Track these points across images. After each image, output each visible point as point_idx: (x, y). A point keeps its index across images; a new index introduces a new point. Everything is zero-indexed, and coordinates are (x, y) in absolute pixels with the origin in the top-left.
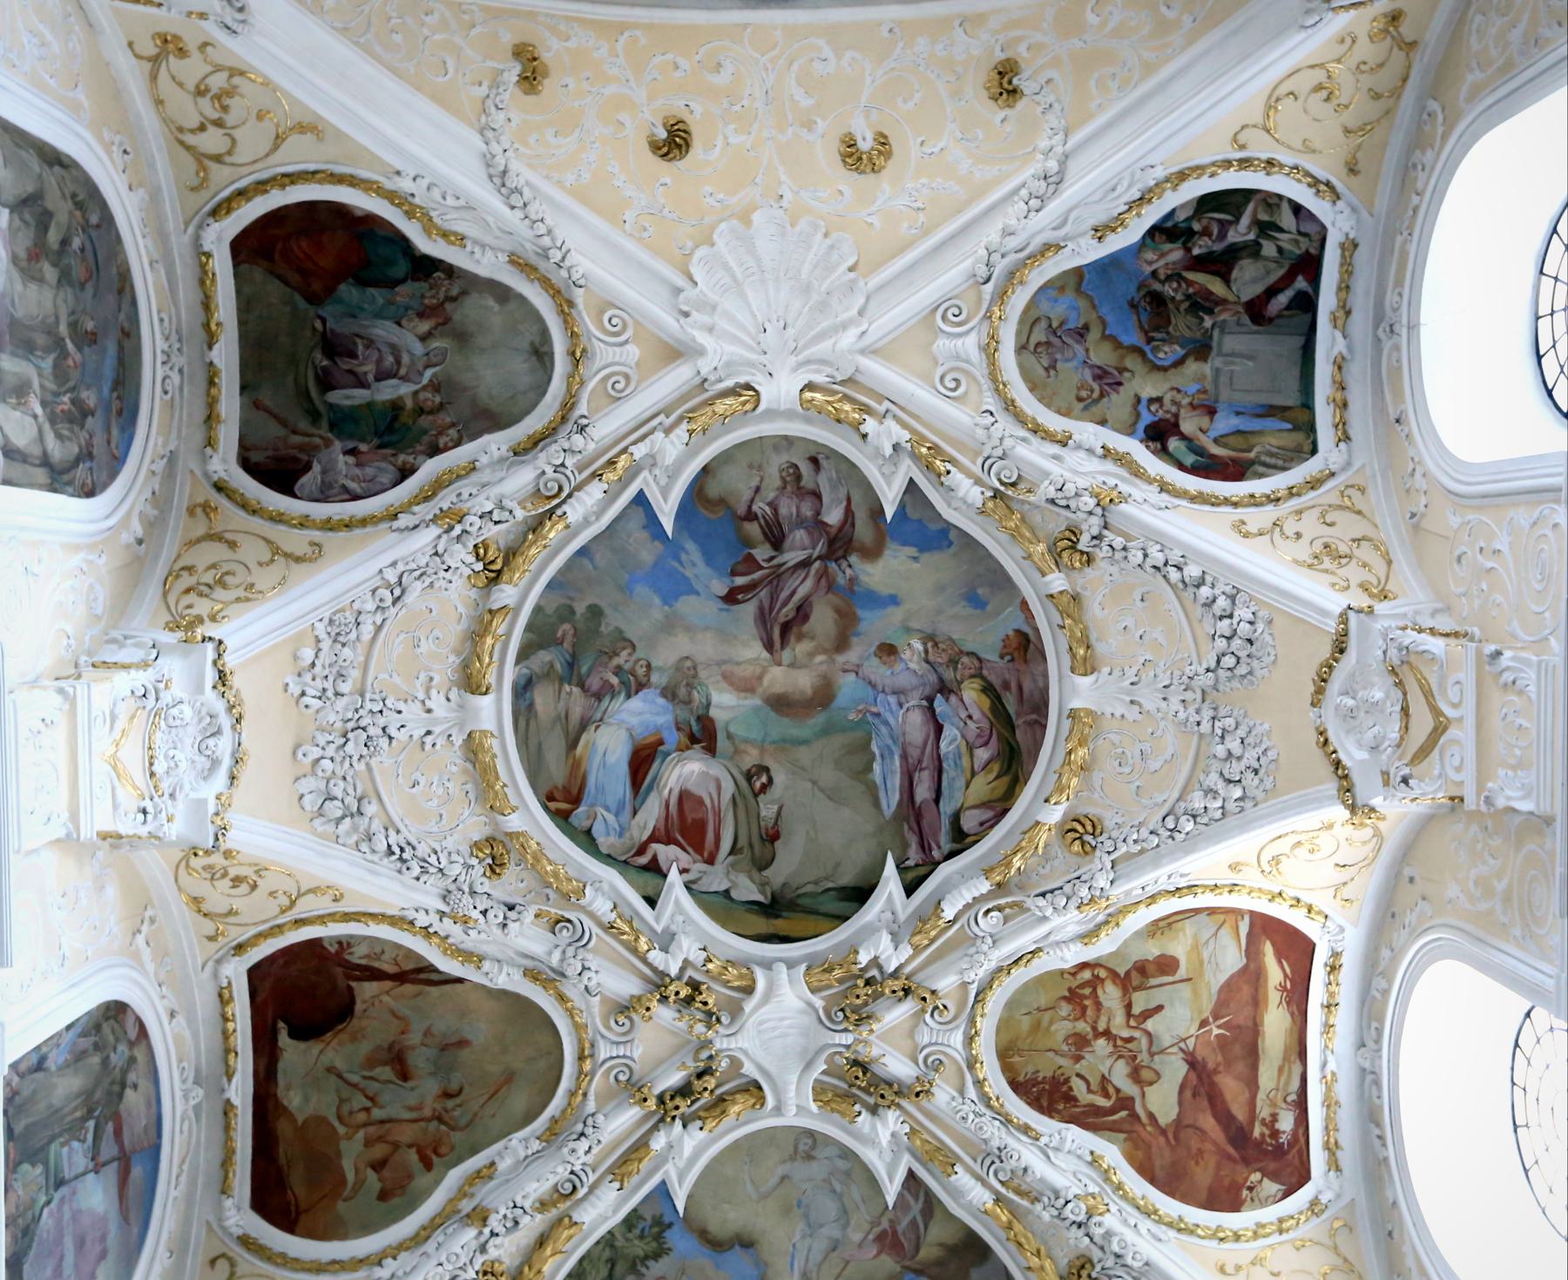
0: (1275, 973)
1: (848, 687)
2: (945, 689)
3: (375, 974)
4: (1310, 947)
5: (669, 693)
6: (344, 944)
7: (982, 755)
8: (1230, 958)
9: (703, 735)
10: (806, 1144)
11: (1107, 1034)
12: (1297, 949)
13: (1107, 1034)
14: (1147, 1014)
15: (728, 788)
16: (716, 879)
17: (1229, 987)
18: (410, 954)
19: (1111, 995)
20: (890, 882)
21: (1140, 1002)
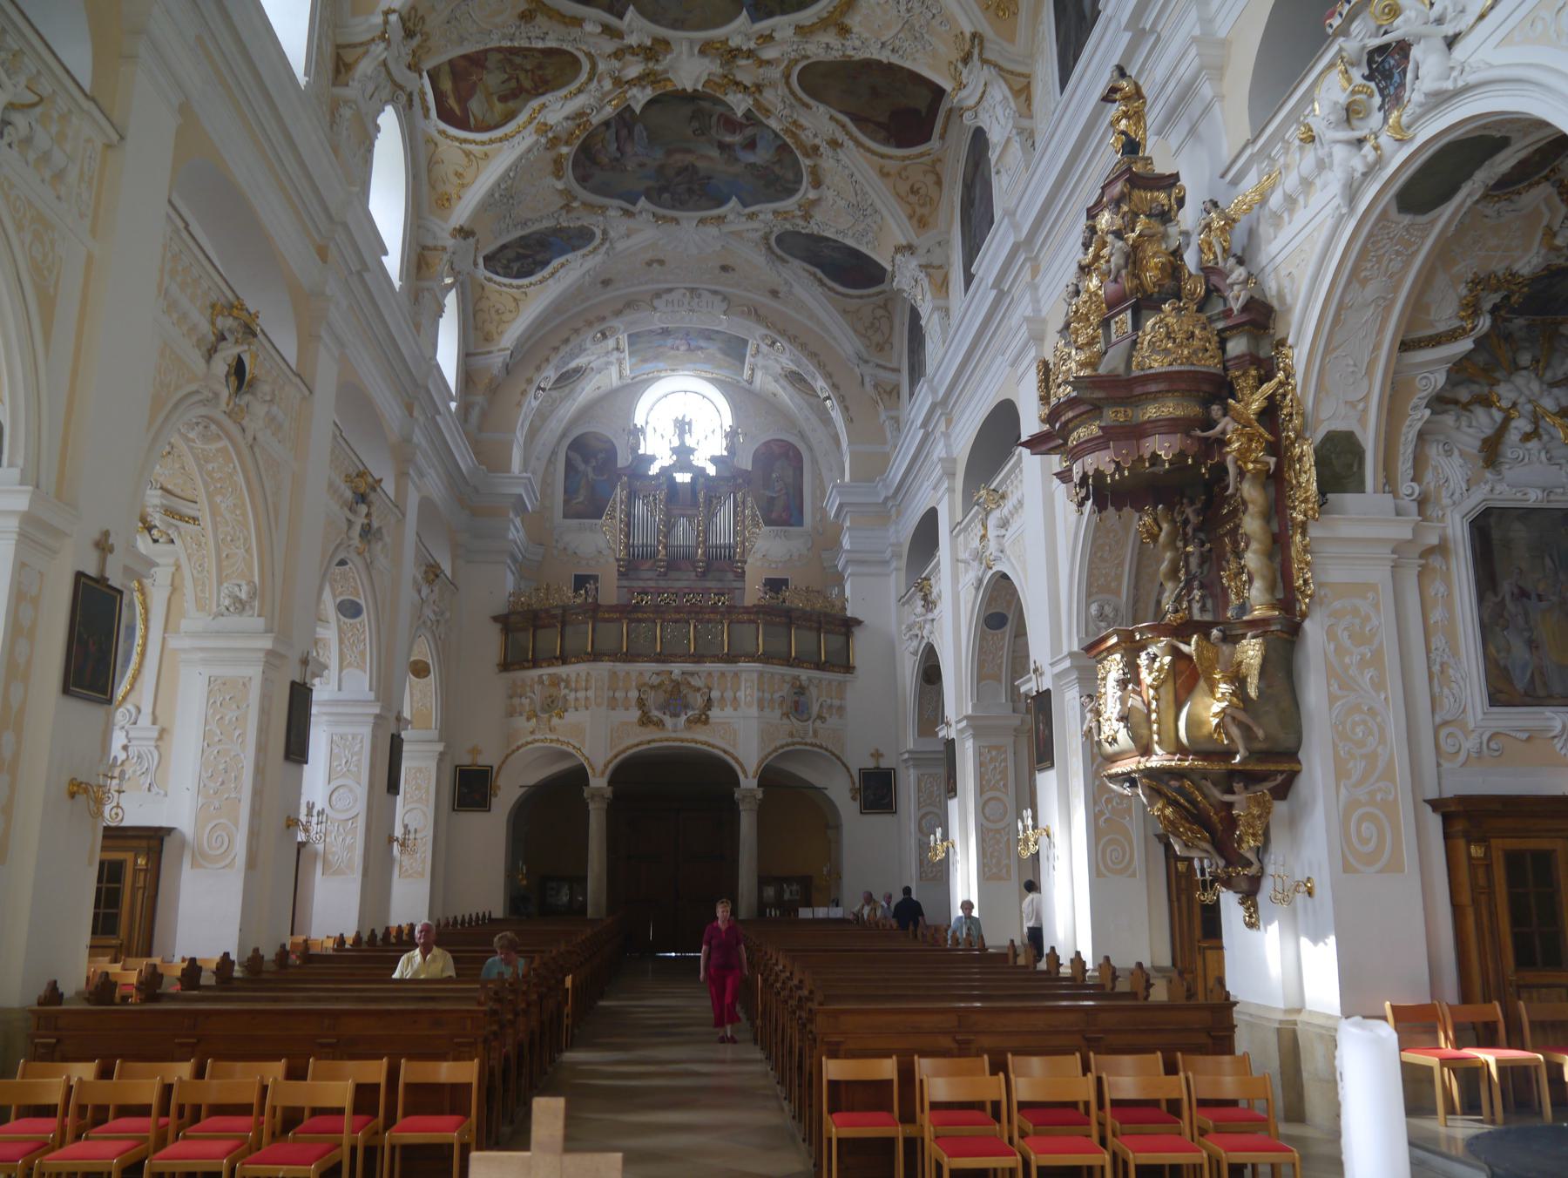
0: (452, 102)
1: (659, 154)
2: (617, 160)
3: (878, 124)
4: (441, 116)
5: (737, 160)
6: (886, 142)
7: (599, 146)
8: (475, 106)
9: (722, 146)
10: (677, 24)
11: (527, 71)
12: (445, 115)
13: (527, 71)
14: (509, 80)
15: (713, 132)
16: (720, 109)
17: (470, 95)
18: (860, 129)
19: (527, 84)
20: (638, 111)
21: (513, 84)
